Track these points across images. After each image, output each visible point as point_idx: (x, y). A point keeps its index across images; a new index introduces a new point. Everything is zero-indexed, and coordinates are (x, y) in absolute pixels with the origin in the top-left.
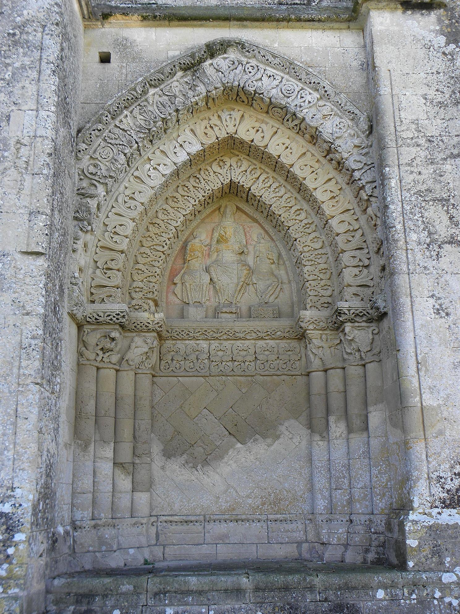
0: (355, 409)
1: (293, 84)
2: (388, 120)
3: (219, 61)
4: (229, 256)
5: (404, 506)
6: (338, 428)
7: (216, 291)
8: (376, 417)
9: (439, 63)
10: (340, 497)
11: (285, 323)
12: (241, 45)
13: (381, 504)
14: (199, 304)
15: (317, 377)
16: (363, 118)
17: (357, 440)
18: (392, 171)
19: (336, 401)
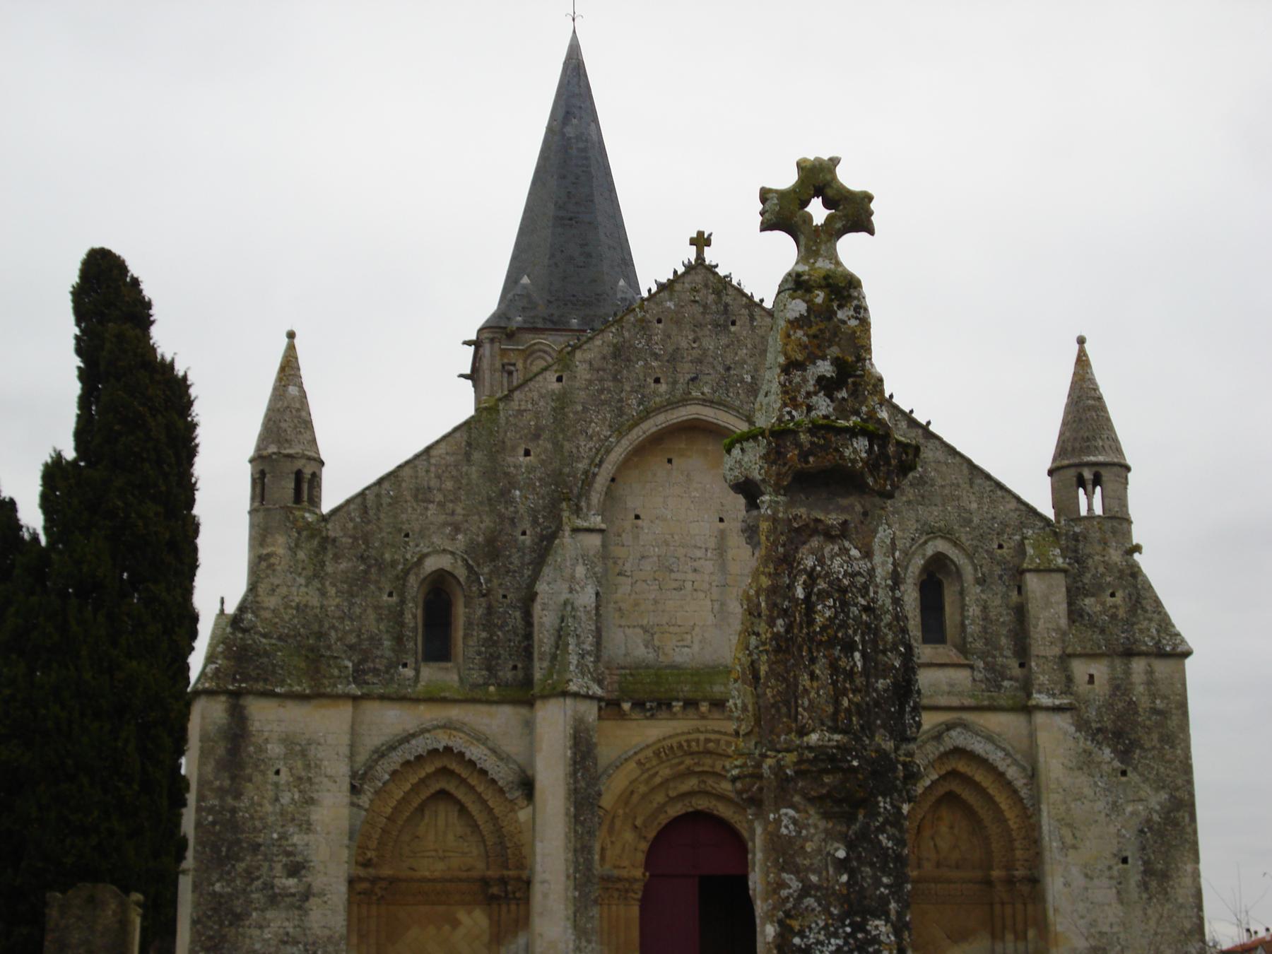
2: (1043, 778)
3: (953, 733)
4: (944, 829)
7: (937, 852)
8: (1031, 934)
9: (1071, 744)
12: (965, 726)
14: (928, 859)
15: (997, 908)
16: (1029, 768)
17: (1021, 946)
18: (1044, 807)
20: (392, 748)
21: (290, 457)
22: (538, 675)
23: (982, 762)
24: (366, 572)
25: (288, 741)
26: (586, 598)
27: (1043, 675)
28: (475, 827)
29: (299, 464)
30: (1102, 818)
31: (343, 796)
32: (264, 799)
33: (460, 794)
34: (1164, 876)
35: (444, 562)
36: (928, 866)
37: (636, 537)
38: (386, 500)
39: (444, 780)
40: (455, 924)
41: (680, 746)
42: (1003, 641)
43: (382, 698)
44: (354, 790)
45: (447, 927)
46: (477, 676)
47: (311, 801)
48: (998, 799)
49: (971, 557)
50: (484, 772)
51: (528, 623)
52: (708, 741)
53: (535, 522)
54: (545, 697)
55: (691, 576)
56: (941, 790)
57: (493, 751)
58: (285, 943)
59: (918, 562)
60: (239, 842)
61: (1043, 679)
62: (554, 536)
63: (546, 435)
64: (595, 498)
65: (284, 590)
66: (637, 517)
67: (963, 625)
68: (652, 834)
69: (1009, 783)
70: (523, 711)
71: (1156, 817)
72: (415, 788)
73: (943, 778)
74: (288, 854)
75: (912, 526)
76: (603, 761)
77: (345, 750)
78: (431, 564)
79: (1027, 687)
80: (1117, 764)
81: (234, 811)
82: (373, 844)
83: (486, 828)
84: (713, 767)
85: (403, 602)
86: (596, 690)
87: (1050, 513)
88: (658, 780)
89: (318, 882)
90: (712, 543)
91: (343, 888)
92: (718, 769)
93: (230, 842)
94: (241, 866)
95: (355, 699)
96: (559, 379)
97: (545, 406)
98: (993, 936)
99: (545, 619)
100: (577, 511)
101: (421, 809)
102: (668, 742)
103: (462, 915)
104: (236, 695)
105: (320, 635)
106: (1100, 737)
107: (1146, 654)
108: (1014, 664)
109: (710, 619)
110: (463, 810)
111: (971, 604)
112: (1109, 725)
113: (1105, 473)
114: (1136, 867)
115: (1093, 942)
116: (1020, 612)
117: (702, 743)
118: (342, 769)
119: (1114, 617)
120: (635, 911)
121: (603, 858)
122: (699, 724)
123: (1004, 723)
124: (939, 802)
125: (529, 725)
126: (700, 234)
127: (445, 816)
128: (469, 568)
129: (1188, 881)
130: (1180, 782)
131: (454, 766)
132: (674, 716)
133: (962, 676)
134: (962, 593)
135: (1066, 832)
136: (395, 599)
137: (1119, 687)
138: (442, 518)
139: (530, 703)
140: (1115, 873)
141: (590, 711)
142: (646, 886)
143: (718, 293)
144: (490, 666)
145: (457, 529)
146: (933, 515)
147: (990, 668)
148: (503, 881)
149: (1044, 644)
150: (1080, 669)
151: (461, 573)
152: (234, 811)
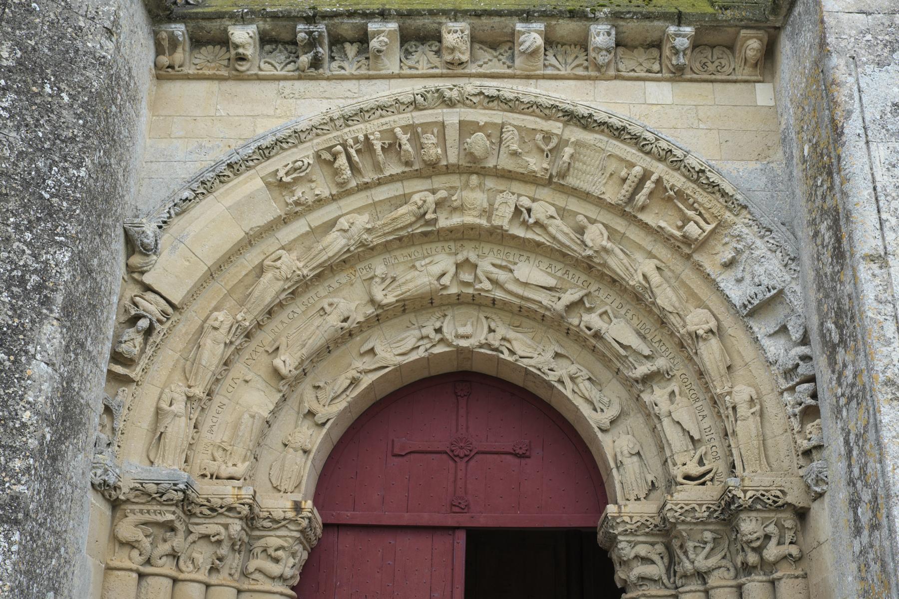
41: (393, 147)
84: (488, 212)
92: (503, 218)
102: (359, 130)
117: (452, 135)
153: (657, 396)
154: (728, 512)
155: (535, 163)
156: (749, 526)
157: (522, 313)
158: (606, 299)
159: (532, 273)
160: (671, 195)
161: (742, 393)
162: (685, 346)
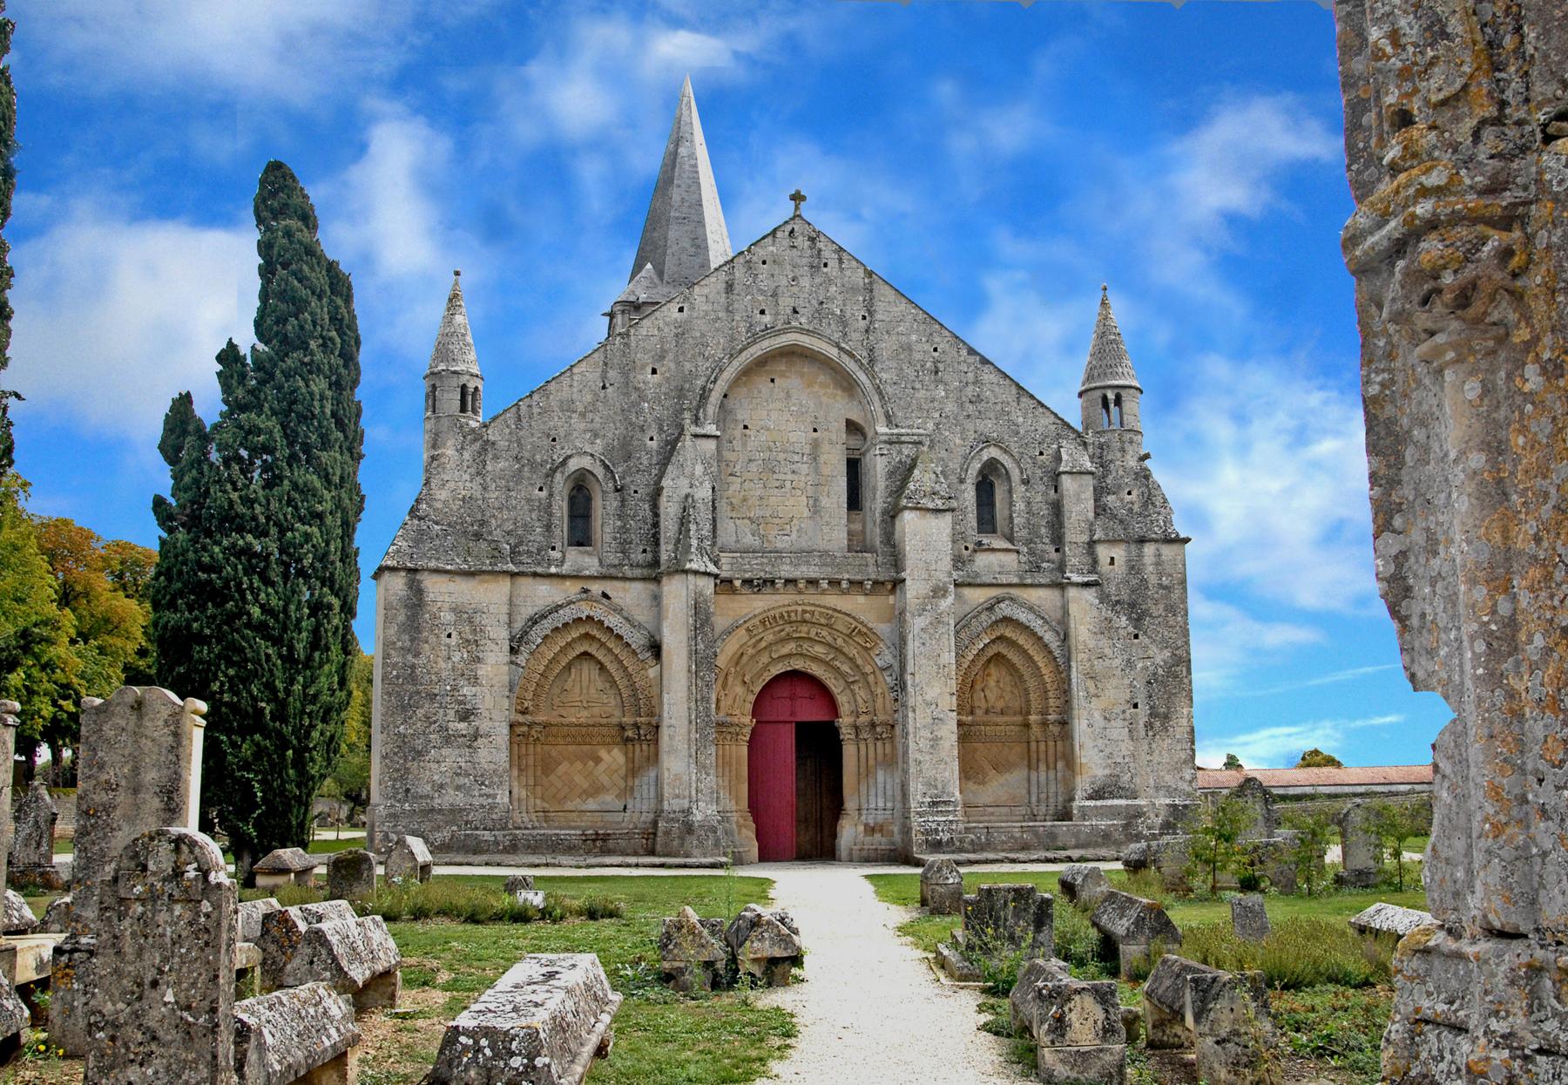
0: (1051, 759)
1: (1031, 616)
2: (1073, 641)
3: (1002, 605)
4: (992, 683)
5: (1072, 799)
6: (1043, 767)
8: (1060, 765)
9: (1095, 613)
10: (1043, 796)
11: (1019, 719)
13: (1060, 799)
15: (1033, 745)
18: (1073, 664)
19: (1042, 756)
20: (544, 617)
21: (455, 372)
22: (664, 557)
23: (1025, 628)
24: (520, 470)
25: (457, 610)
26: (703, 493)
27: (1074, 557)
28: (614, 683)
29: (464, 379)
30: (1118, 672)
31: (503, 655)
32: (440, 658)
33: (600, 655)
34: (1166, 717)
35: (586, 462)
36: (979, 712)
37: (744, 444)
38: (536, 410)
39: (588, 642)
40: (598, 760)
41: (782, 616)
42: (1043, 530)
43: (535, 575)
44: (513, 651)
45: (591, 763)
46: (613, 558)
47: (478, 660)
48: (1036, 658)
49: (1018, 463)
50: (620, 637)
51: (656, 515)
52: (804, 612)
53: (661, 429)
54: (670, 574)
55: (790, 477)
56: (990, 652)
57: (627, 619)
58: (458, 775)
59: (976, 466)
60: (418, 693)
61: (1074, 561)
62: (677, 440)
63: (671, 356)
64: (712, 408)
65: (452, 485)
66: (746, 427)
67: (1011, 517)
68: (757, 689)
69: (1046, 646)
70: (652, 586)
71: (1160, 671)
72: (563, 650)
73: (993, 641)
74: (461, 703)
75: (971, 435)
76: (718, 630)
77: (504, 618)
78: (574, 465)
79: (1061, 568)
80: (1131, 629)
81: (413, 667)
82: (529, 695)
83: (622, 683)
85: (551, 495)
86: (712, 568)
87: (1080, 428)
88: (763, 644)
89: (484, 726)
90: (807, 451)
91: (506, 731)
92: (812, 635)
93: (410, 689)
94: (420, 713)
95: (513, 575)
96: (681, 310)
97: (669, 332)
98: (1029, 767)
99: (670, 509)
100: (696, 421)
101: (569, 667)
103: (603, 753)
104: (415, 571)
105: (483, 523)
106: (1118, 608)
107: (1156, 541)
108: (1051, 549)
109: (806, 513)
110: (602, 668)
111: (1020, 502)
112: (1125, 597)
113: (1124, 393)
114: (1143, 710)
115: (1107, 772)
116: (1057, 508)
118: (502, 634)
119: (1131, 510)
120: (745, 749)
121: (718, 708)
122: (798, 598)
123: (1043, 597)
124: (989, 661)
125: (657, 599)
126: (798, 192)
127: (587, 671)
128: (606, 467)
129: (1184, 722)
130: (1179, 643)
131: (595, 632)
132: (776, 591)
133: (1010, 559)
134: (1010, 491)
135: (1090, 683)
136: (544, 494)
137: (1134, 568)
138: (582, 426)
139: (657, 580)
140: (1127, 715)
141: (707, 586)
142: (753, 730)
143: (812, 240)
144: (624, 547)
145: (596, 436)
146: (988, 427)
147: (1032, 552)
148: (636, 726)
149: (1075, 534)
150: (1103, 552)
151: (599, 472)
152: (413, 667)
153: (855, 687)
154: (873, 725)
155: (823, 621)
156: (879, 729)
157: (815, 659)
158: (842, 658)
159: (819, 650)
160: (860, 632)
161: (879, 691)
162: (865, 675)
